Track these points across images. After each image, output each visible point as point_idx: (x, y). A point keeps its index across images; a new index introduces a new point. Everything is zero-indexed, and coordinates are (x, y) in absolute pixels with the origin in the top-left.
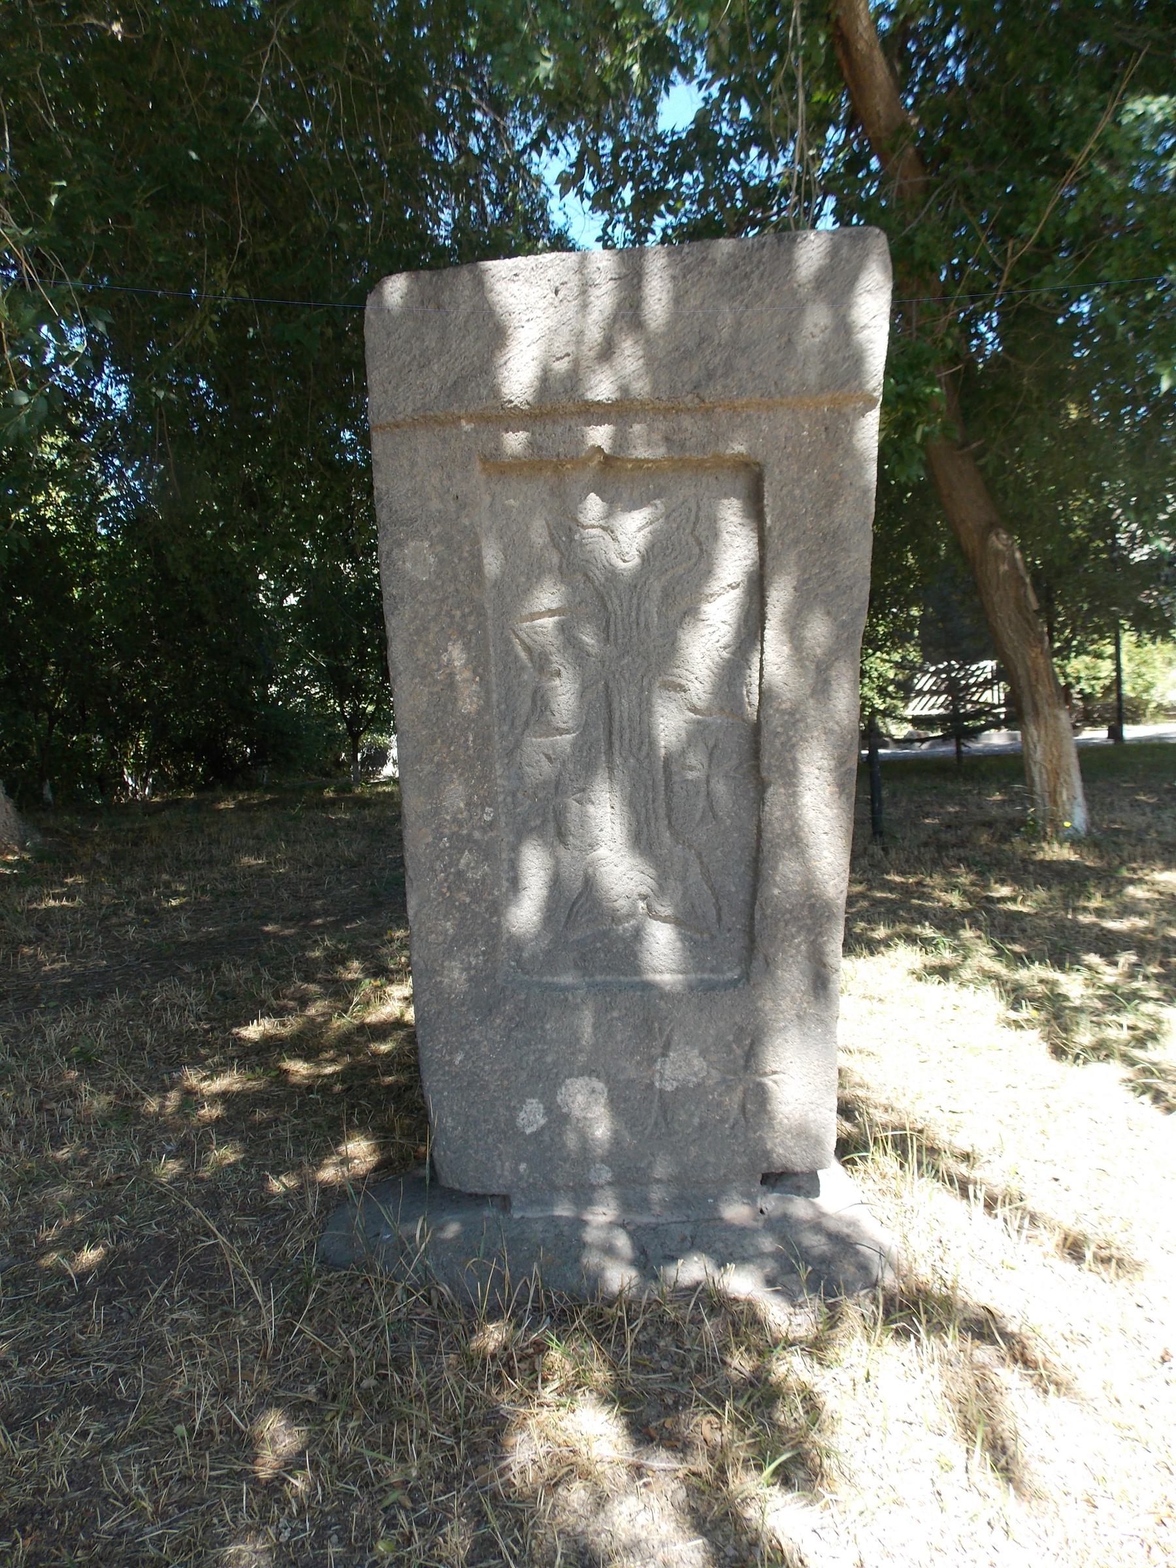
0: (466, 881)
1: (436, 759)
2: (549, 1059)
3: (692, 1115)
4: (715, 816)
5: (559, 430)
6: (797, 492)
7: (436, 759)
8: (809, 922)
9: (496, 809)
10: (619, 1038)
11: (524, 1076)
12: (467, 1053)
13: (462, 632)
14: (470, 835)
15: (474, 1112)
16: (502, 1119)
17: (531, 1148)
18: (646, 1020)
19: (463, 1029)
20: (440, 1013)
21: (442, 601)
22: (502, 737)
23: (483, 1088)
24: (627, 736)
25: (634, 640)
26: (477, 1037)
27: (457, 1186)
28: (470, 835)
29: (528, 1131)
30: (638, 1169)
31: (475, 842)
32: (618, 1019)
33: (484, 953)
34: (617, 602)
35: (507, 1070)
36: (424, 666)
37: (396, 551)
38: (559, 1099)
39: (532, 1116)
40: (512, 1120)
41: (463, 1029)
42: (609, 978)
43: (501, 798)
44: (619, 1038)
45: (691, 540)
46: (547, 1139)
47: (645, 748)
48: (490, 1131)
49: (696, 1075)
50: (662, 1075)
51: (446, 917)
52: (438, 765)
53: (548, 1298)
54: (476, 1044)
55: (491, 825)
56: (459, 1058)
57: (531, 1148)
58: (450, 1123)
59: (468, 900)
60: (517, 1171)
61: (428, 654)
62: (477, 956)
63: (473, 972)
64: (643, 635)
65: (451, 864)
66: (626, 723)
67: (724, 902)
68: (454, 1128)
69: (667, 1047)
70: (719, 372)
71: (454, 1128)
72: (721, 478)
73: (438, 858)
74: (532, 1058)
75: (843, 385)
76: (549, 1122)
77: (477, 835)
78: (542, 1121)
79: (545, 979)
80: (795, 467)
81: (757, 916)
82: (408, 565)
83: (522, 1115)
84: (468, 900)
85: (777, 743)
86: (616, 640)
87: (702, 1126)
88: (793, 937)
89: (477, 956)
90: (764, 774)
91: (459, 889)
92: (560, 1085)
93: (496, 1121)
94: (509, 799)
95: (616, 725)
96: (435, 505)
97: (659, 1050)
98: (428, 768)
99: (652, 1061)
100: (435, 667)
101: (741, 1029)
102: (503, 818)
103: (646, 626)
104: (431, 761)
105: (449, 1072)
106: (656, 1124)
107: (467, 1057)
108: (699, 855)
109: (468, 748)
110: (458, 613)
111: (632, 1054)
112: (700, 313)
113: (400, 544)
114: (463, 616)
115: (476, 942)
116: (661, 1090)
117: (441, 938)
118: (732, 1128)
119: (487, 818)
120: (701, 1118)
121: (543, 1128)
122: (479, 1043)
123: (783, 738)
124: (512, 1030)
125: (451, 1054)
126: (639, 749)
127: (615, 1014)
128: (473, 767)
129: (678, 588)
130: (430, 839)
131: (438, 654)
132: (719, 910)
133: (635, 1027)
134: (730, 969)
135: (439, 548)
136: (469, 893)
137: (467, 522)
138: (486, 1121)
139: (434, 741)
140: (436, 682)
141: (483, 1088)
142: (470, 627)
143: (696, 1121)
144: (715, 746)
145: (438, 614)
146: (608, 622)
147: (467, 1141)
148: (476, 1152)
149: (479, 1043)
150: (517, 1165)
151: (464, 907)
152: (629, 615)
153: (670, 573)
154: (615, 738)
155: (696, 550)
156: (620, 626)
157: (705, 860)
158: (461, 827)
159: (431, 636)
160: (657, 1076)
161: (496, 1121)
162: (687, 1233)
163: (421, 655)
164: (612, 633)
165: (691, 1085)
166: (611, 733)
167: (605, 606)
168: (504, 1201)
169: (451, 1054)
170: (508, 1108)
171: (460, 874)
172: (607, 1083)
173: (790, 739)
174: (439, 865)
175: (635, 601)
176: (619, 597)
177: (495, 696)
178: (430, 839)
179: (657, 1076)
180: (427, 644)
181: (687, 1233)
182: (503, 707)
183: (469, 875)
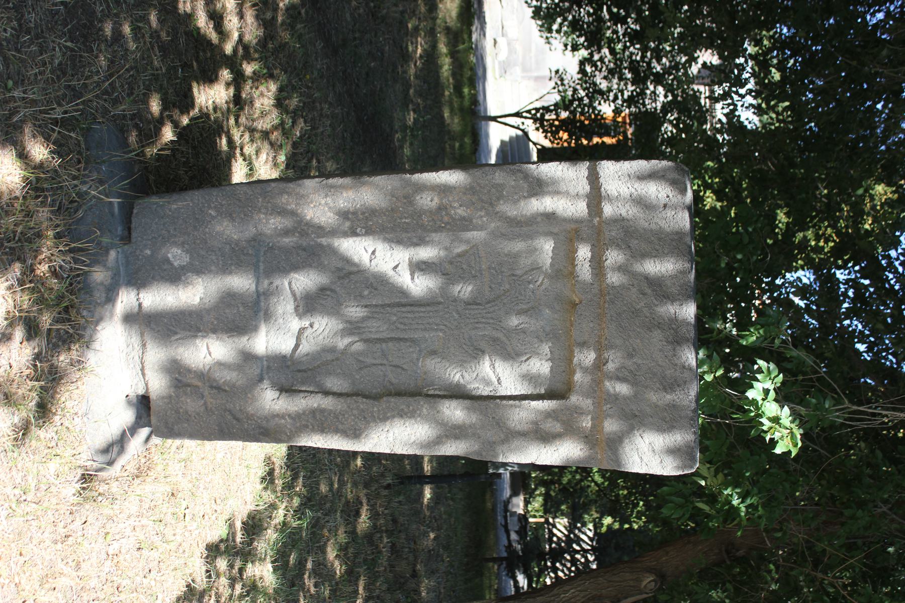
4: (361, 369)
10: (227, 311)
15: (181, 221)
16: (177, 240)
20: (240, 201)
23: (195, 227)
24: (409, 315)
27: (135, 211)
32: (238, 311)
34: (491, 310)
35: (206, 243)
44: (227, 311)
46: (165, 267)
47: (402, 327)
48: (169, 232)
53: (78, 275)
67: (309, 373)
68: (170, 210)
71: (170, 210)
72: (564, 374)
74: (214, 258)
75: (609, 446)
76: (176, 268)
78: (176, 264)
79: (261, 264)
80: (565, 418)
85: (403, 407)
90: (385, 399)
95: (416, 309)
100: (450, 199)
103: (476, 328)
105: (204, 206)
108: (337, 359)
109: (401, 219)
111: (217, 319)
121: (172, 265)
126: (401, 323)
127: (241, 309)
129: (498, 347)
132: (305, 371)
138: (175, 229)
141: (195, 227)
144: (403, 369)
145: (482, 201)
146: (479, 304)
148: (156, 223)
152: (483, 317)
153: (508, 343)
154: (408, 308)
156: (476, 312)
157: (335, 363)
161: (175, 236)
164: (472, 307)
166: (411, 305)
167: (488, 303)
168: (127, 238)
169: (215, 207)
170: (183, 243)
175: (491, 321)
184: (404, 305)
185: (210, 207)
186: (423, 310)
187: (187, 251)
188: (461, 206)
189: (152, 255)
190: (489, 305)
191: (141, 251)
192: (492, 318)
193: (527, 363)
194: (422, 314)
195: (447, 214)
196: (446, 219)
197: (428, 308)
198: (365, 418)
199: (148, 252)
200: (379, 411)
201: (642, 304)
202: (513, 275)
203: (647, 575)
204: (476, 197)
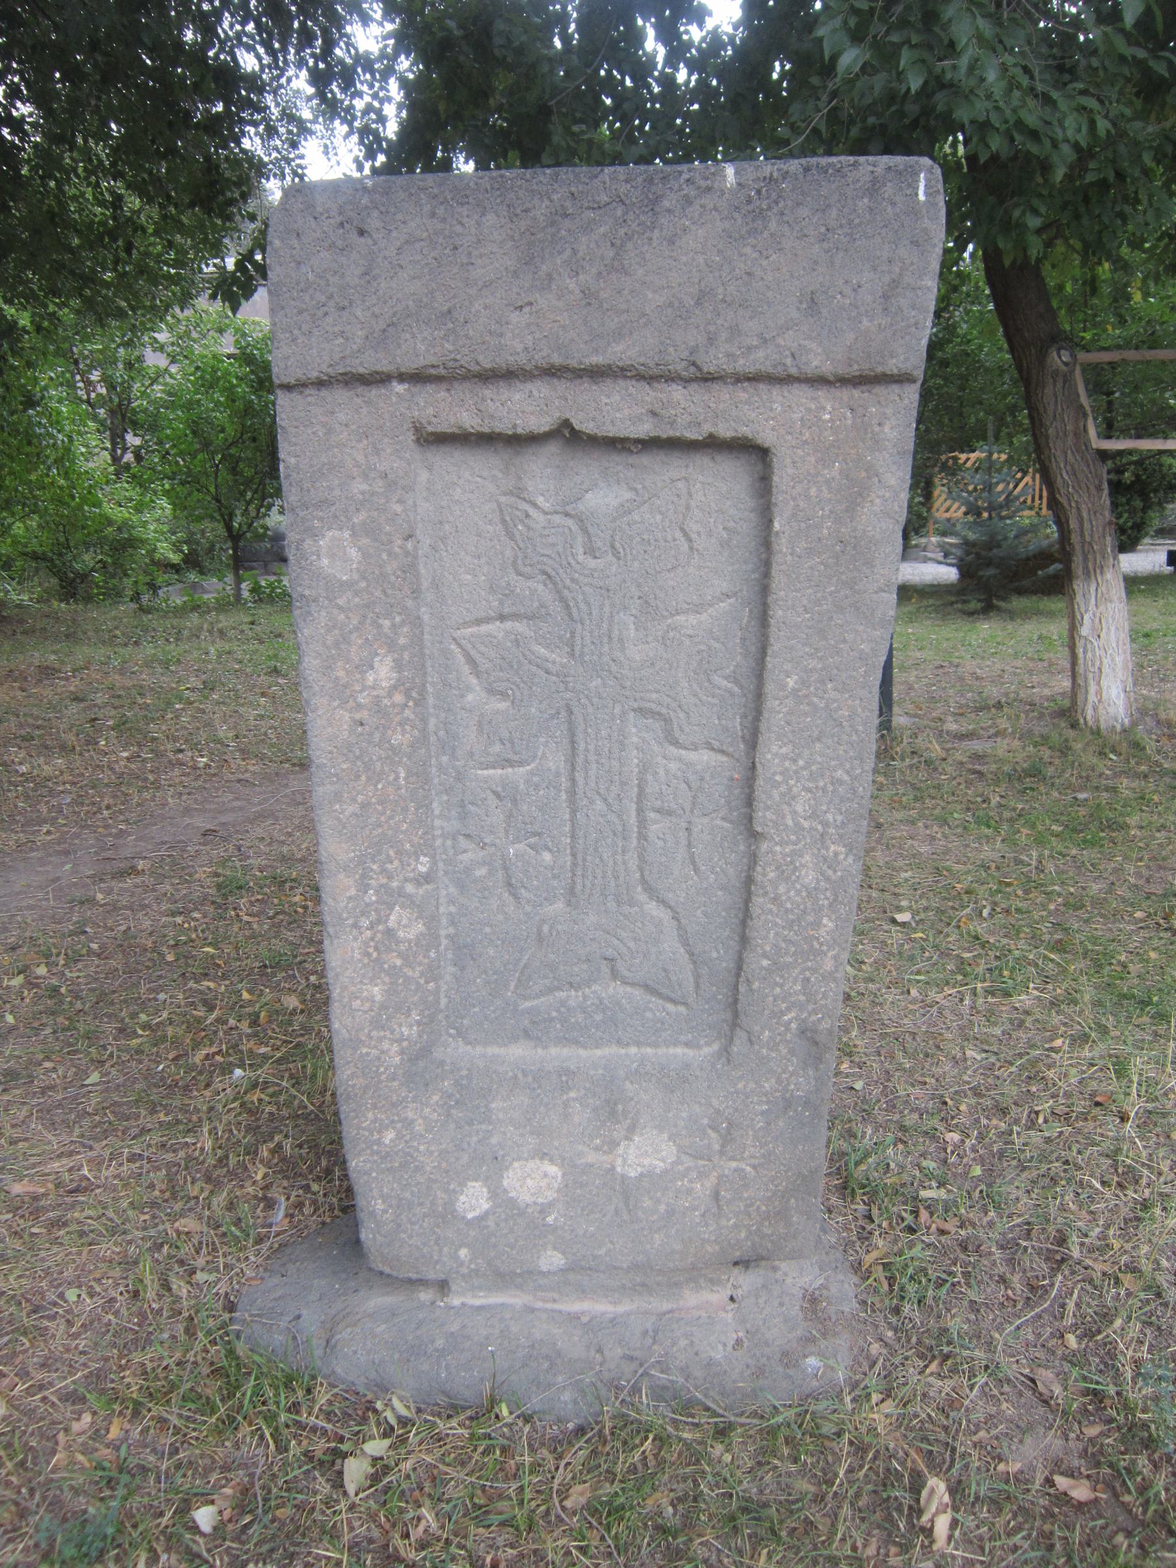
0: (398, 942)
1: (360, 798)
2: (494, 1141)
3: (658, 1201)
5: (517, 396)
6: (813, 491)
7: (360, 798)
8: (802, 998)
9: (433, 857)
11: (465, 1158)
12: (399, 1132)
13: (391, 646)
14: (401, 888)
15: (408, 1195)
17: (472, 1233)
18: (607, 1101)
19: (394, 1105)
21: (367, 606)
22: (440, 768)
23: (417, 1169)
25: (606, 659)
26: (410, 1114)
28: (401, 888)
29: (470, 1216)
30: (595, 1257)
31: (409, 896)
33: (419, 1023)
36: (345, 686)
37: (308, 541)
38: (505, 1183)
39: (474, 1200)
40: (450, 1204)
41: (394, 1105)
42: (565, 1051)
43: (438, 842)
44: (576, 1119)
45: (678, 534)
48: (425, 1215)
49: (663, 1160)
50: (625, 1161)
51: (373, 981)
52: (364, 806)
54: (409, 1124)
55: (427, 878)
56: (389, 1136)
57: (472, 1233)
58: (380, 1205)
59: (399, 962)
60: (457, 1258)
61: (348, 672)
62: (411, 1026)
63: (405, 1044)
64: (617, 654)
65: (379, 921)
66: (592, 758)
67: (704, 971)
69: (632, 1129)
70: (724, 336)
73: (363, 914)
74: (475, 1139)
77: (410, 888)
78: (486, 1206)
81: (742, 988)
82: (325, 561)
83: (462, 1198)
84: (399, 962)
86: (582, 654)
87: (670, 1212)
88: (783, 1013)
89: (411, 1026)
91: (389, 950)
92: (507, 1168)
93: (433, 1203)
94: (449, 843)
95: (580, 760)
96: (359, 487)
97: (623, 1133)
98: (350, 809)
99: (614, 1144)
101: (718, 1112)
102: (441, 865)
103: (621, 640)
104: (354, 800)
105: (378, 1153)
106: (617, 1212)
107: (400, 1136)
110: (387, 623)
112: (700, 259)
113: (315, 535)
114: (393, 625)
115: (409, 1010)
116: (623, 1176)
117: (368, 1005)
118: (703, 1215)
119: (423, 869)
120: (667, 1205)
121: (487, 1213)
122: (413, 1121)
123: (783, 789)
124: (451, 1107)
125: (379, 1132)
127: (572, 1094)
128: (405, 810)
130: (353, 892)
131: (363, 673)
133: (595, 1110)
134: (708, 1044)
135: (365, 541)
136: (400, 955)
137: (398, 508)
138: (421, 1204)
139: (358, 777)
140: (359, 706)
141: (417, 1169)
142: (402, 641)
143: (662, 1208)
146: (573, 634)
147: (399, 1226)
148: (410, 1237)
149: (413, 1121)
150: (457, 1250)
151: (393, 972)
152: (599, 626)
154: (579, 777)
155: (685, 547)
156: (588, 640)
158: (390, 878)
159: (354, 649)
160: (619, 1161)
162: (649, 1326)
163: (341, 674)
165: (658, 1171)
167: (570, 615)
169: (379, 1132)
170: (447, 1191)
171: (389, 932)
172: (562, 1166)
173: (790, 789)
174: (365, 923)
175: (607, 609)
176: (588, 604)
177: (432, 721)
178: (353, 892)
179: (619, 1161)
180: (348, 661)
181: (649, 1326)
182: (442, 733)
183: (401, 934)
184: (573, 780)
185: (379, 1142)
186: (582, 745)
187: (462, 1184)
188: (372, 667)
189: (468, 1246)
190: (574, 611)
191: (462, 1264)
192: (602, 607)
193: (694, 536)
194: (591, 747)
195: (390, 696)
196: (399, 698)
197: (580, 736)
198: (796, 868)
199: (463, 1253)
200: (780, 844)
201: (572, 284)
202: (514, 563)
203: (1049, 360)
204: (354, 636)
